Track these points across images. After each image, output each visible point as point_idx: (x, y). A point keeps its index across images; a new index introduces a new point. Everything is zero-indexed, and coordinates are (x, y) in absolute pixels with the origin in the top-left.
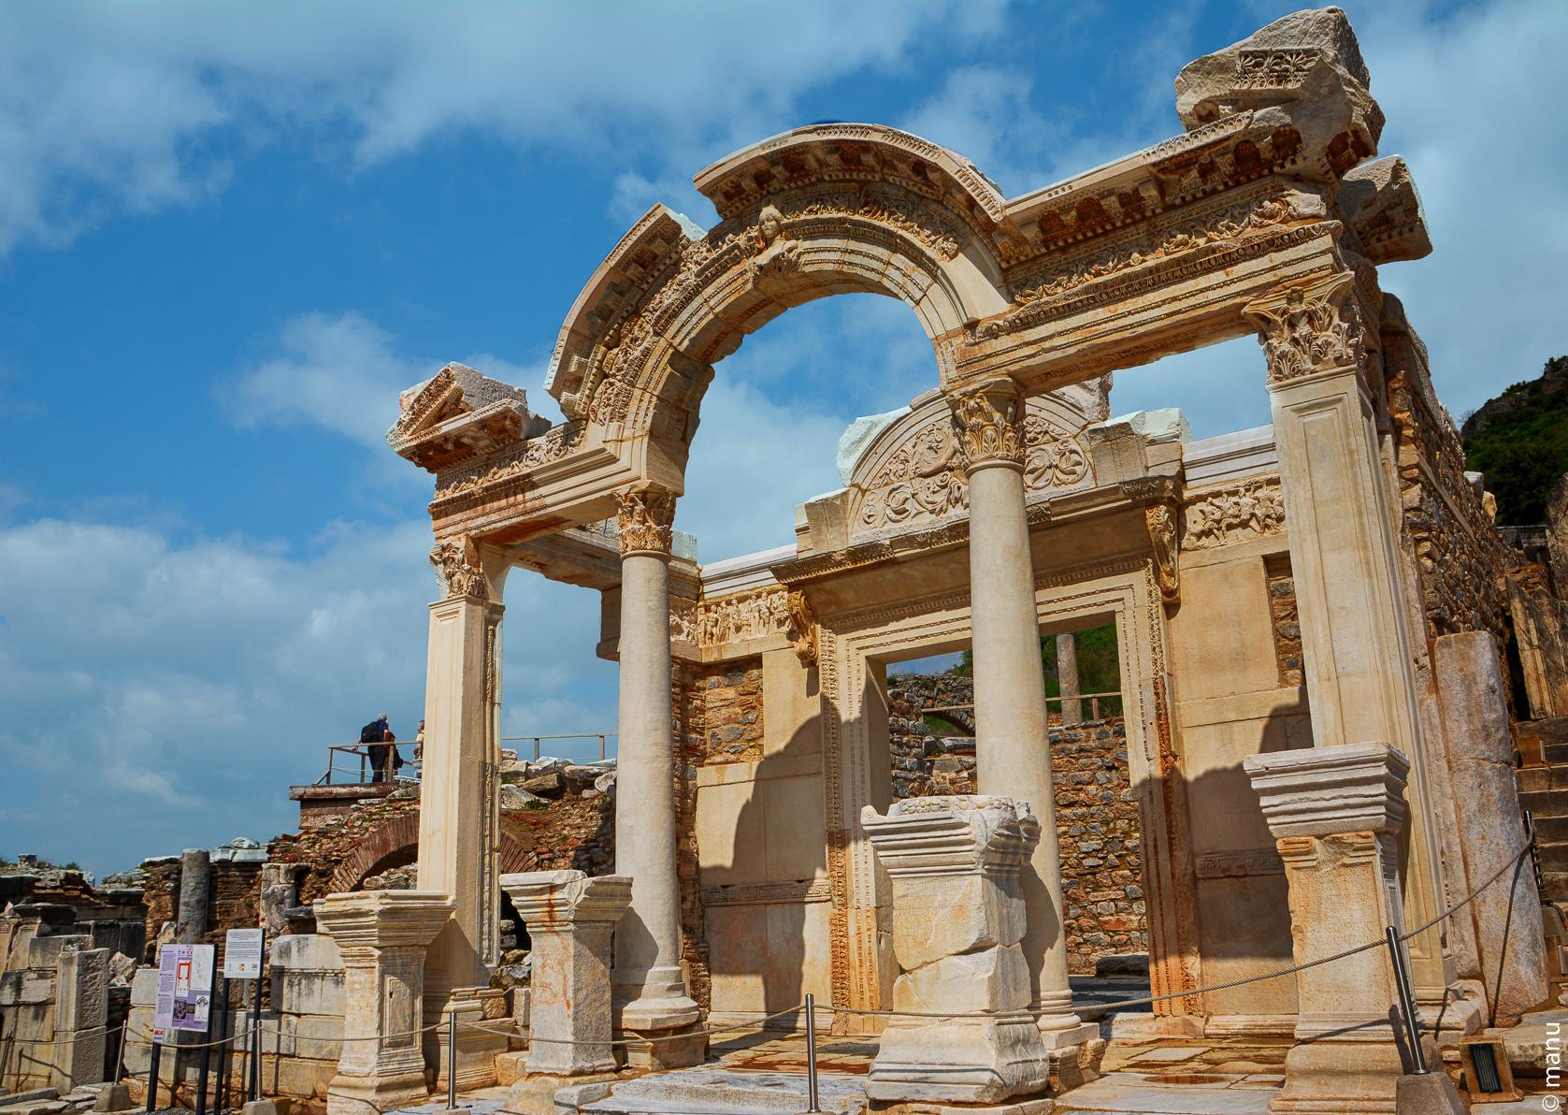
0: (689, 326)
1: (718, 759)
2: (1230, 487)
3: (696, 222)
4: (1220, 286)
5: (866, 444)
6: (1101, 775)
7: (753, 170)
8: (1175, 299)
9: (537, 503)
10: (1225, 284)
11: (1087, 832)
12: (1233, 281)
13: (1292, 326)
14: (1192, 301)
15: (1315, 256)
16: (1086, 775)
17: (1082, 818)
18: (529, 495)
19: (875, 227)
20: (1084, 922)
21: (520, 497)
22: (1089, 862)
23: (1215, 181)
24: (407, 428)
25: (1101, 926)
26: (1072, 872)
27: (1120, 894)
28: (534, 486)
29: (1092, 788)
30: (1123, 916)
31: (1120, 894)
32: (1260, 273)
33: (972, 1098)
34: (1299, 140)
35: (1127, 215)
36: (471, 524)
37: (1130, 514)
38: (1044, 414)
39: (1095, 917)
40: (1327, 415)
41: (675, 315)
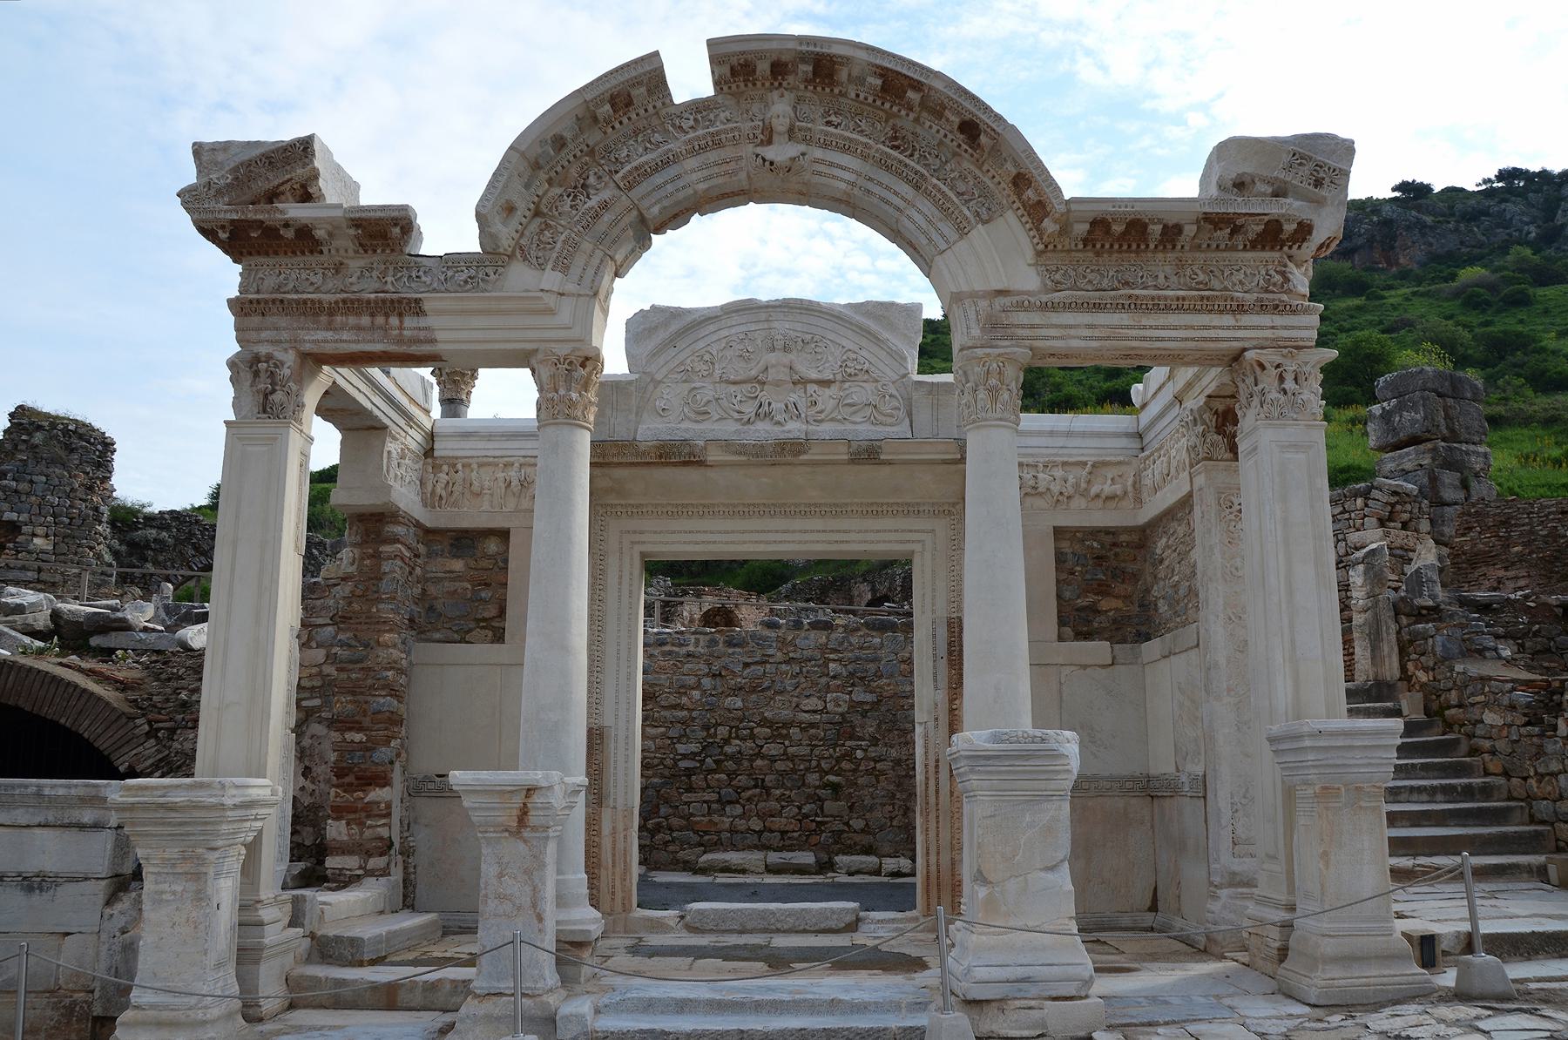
0: (662, 193)
1: (437, 636)
2: (1030, 460)
3: (691, 80)
4: (1228, 328)
5: (662, 335)
6: (707, 682)
7: (774, 57)
8: (1192, 328)
9: (422, 334)
10: (1234, 328)
11: (685, 735)
12: (1240, 328)
13: (1281, 379)
14: (1205, 334)
15: (1306, 328)
16: (692, 681)
17: (683, 722)
18: (409, 322)
19: (906, 165)
20: (675, 821)
21: (394, 321)
22: (683, 764)
23: (1239, 240)
24: (219, 193)
25: (690, 826)
26: (666, 772)
27: (715, 797)
28: (420, 312)
29: (696, 694)
30: (716, 818)
31: (715, 797)
32: (1261, 328)
33: (1074, 993)
34: (1310, 233)
35: (1161, 242)
36: (302, 334)
37: (953, 467)
38: (863, 353)
39: (688, 817)
40: (1302, 456)
41: (647, 175)
